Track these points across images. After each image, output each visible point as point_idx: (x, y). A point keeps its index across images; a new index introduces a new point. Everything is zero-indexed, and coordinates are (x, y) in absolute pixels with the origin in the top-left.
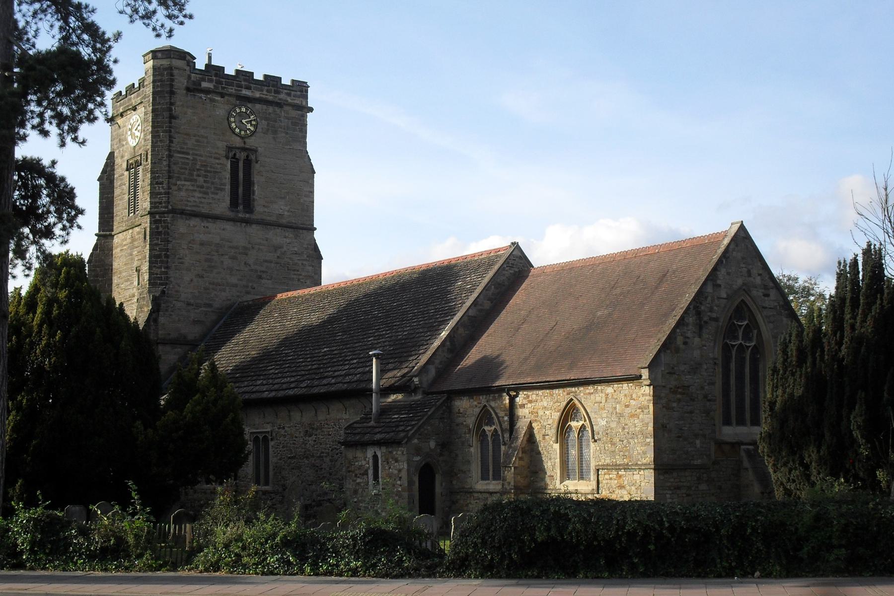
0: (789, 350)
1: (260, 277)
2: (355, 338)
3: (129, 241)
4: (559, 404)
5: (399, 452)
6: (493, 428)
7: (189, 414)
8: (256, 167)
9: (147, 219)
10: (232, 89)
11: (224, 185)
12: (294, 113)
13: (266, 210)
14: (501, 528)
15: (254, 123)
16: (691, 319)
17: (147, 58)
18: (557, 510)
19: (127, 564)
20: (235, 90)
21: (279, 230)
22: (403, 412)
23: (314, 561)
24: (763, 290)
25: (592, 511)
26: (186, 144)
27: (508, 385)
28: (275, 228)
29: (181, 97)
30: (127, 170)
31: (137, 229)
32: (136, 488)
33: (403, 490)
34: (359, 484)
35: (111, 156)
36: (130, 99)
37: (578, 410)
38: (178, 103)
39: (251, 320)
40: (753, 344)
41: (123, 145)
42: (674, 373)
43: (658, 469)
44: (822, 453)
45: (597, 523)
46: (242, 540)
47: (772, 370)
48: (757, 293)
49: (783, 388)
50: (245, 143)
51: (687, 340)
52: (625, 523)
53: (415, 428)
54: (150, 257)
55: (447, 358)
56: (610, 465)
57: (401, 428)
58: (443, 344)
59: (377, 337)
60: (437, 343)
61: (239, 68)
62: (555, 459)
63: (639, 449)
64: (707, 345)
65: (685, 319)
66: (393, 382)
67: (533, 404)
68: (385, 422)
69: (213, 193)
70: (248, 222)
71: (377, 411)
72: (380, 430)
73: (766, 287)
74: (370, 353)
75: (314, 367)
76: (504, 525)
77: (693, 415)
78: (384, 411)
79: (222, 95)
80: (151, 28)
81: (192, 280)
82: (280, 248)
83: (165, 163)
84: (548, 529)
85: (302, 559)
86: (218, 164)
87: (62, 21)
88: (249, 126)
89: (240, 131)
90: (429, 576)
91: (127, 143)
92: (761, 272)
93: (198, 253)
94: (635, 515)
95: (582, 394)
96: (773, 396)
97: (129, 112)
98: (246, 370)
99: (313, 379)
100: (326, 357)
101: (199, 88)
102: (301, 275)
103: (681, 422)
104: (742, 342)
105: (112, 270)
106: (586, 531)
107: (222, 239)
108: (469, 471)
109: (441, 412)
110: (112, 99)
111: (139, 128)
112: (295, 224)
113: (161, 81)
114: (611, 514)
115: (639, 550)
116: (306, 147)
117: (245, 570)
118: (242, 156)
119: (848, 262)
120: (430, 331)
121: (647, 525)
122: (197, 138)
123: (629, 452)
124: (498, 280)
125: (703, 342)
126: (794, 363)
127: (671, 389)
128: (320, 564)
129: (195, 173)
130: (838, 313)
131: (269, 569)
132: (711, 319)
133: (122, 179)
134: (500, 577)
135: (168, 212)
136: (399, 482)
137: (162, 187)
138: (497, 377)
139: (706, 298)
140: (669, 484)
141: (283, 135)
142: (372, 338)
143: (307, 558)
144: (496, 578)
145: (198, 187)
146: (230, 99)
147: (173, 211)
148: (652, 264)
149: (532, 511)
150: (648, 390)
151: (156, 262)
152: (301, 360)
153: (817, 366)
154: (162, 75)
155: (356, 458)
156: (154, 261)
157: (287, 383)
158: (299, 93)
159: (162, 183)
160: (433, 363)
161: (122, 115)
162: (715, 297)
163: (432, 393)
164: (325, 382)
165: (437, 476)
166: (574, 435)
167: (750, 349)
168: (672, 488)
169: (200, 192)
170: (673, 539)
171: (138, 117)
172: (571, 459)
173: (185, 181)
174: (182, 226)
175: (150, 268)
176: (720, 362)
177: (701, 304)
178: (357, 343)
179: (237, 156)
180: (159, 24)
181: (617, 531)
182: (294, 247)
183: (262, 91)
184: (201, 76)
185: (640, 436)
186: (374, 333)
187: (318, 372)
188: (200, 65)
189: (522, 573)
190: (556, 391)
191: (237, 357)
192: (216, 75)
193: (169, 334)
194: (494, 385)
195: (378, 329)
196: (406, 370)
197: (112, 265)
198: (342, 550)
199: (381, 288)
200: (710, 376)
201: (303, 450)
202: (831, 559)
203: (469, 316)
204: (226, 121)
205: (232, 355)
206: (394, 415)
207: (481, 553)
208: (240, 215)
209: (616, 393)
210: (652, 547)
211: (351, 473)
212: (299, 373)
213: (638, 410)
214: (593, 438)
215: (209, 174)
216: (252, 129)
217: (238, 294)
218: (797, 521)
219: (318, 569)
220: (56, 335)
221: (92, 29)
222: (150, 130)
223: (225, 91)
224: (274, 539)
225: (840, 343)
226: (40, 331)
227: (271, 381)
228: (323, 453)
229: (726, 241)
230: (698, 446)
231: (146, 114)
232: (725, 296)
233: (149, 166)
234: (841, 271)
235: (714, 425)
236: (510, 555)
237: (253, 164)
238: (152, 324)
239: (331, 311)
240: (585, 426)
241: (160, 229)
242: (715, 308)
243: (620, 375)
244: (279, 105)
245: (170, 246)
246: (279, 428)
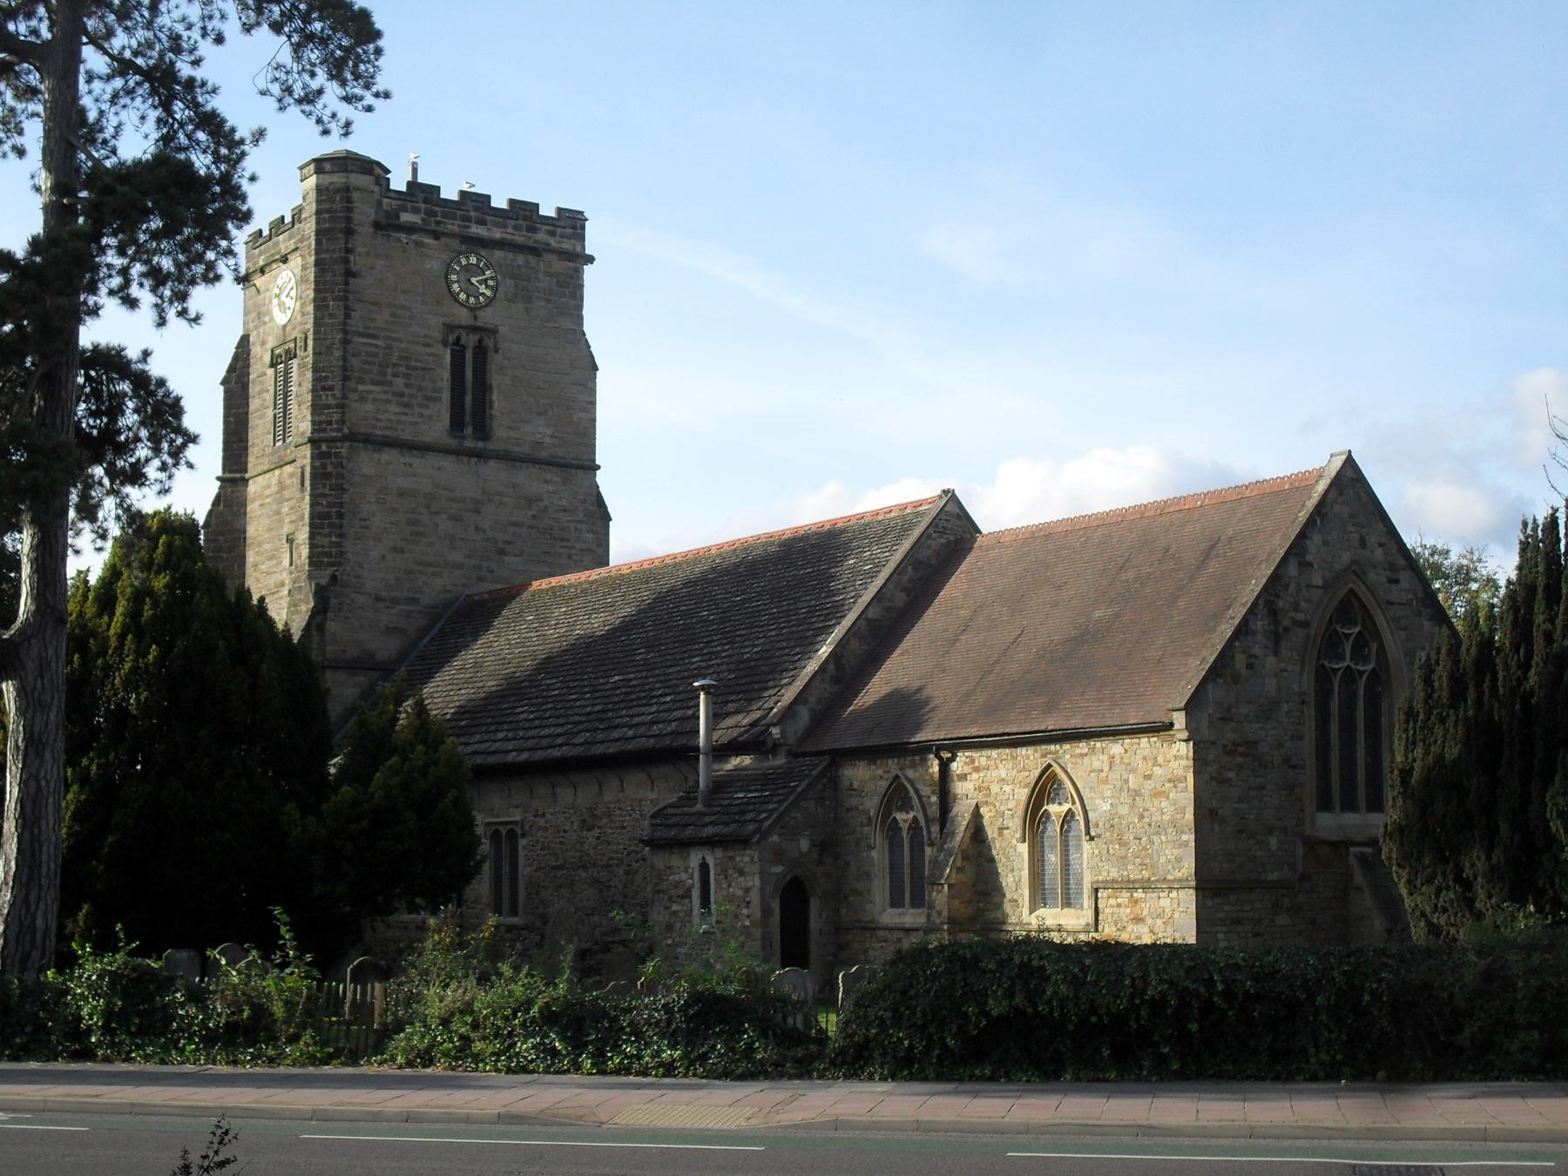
0: (1435, 677)
1: (502, 552)
2: (669, 657)
3: (274, 489)
4: (1027, 774)
5: (746, 858)
6: (911, 816)
7: (380, 792)
8: (495, 361)
9: (307, 451)
10: (453, 224)
11: (439, 390)
12: (561, 266)
13: (512, 434)
14: (928, 991)
15: (491, 283)
16: (1260, 623)
17: (306, 171)
18: (1025, 960)
19: (271, 1052)
20: (459, 226)
21: (534, 470)
22: (752, 788)
23: (597, 1049)
24: (1388, 573)
25: (1088, 962)
26: (374, 320)
27: (938, 740)
28: (527, 467)
29: (364, 239)
30: (273, 365)
31: (288, 469)
32: (288, 919)
33: (753, 924)
34: (675, 913)
35: (244, 343)
36: (277, 243)
37: (1060, 784)
38: (360, 249)
39: (486, 626)
40: (1370, 667)
41: (265, 323)
42: (1231, 719)
43: (1203, 889)
44: (1495, 860)
45: (1095, 983)
46: (472, 1012)
47: (1406, 713)
48: (1376, 577)
49: (1424, 744)
50: (475, 318)
51: (1253, 660)
52: (1147, 984)
53: (775, 816)
54: (312, 517)
55: (830, 693)
56: (1117, 882)
57: (749, 816)
58: (823, 668)
59: (707, 657)
60: (812, 667)
61: (465, 188)
62: (1021, 870)
63: (1170, 853)
64: (1289, 669)
65: (1251, 624)
66: (735, 735)
67: (982, 774)
68: (721, 805)
69: (421, 406)
70: (481, 456)
71: (707, 787)
72: (713, 818)
73: (1392, 567)
74: (696, 684)
75: (596, 709)
76: (931, 987)
77: (1264, 792)
78: (720, 786)
79: (436, 235)
80: (314, 118)
81: (383, 557)
82: (536, 501)
83: (337, 354)
84: (1010, 995)
85: (578, 1045)
86: (429, 355)
87: (161, 109)
88: (482, 289)
89: (468, 297)
90: (799, 1077)
91: (272, 320)
92: (1384, 540)
93: (395, 510)
94: (1164, 969)
95: (1067, 757)
96: (1407, 758)
97: (274, 266)
98: (478, 714)
99: (596, 730)
100: (618, 692)
101: (397, 222)
102: (573, 548)
103: (1244, 806)
104: (1353, 666)
105: (245, 539)
106: (1076, 997)
107: (436, 486)
108: (869, 891)
109: (820, 787)
110: (246, 243)
111: (293, 293)
112: (564, 458)
113: (329, 211)
114: (1122, 967)
115: (1170, 1031)
116: (581, 325)
117: (477, 1064)
118: (470, 340)
119: (1541, 521)
120: (799, 646)
121: (1185, 988)
122: (394, 310)
123: (1152, 859)
124: (920, 556)
125: (1282, 665)
126: (1445, 700)
127: (1225, 746)
128: (609, 1055)
129: (390, 371)
130: (1522, 611)
131: (519, 1062)
132: (1296, 623)
133: (262, 382)
134: (925, 1079)
135: (345, 438)
136: (745, 911)
137: (333, 396)
138: (918, 727)
139: (1288, 585)
140: (1222, 915)
141: (543, 303)
142: (698, 658)
143: (586, 1044)
144: (917, 1080)
145: (394, 394)
146: (449, 241)
147: (352, 437)
148: (1189, 528)
149: (982, 962)
150: (1184, 750)
151: (321, 526)
152: (574, 696)
153: (1485, 707)
154: (333, 201)
155: (670, 867)
156: (318, 522)
157: (550, 736)
158: (569, 231)
159: (331, 389)
160: (805, 702)
161: (262, 271)
162: (1304, 585)
163: (804, 755)
164: (616, 734)
165: (812, 901)
166: (1054, 829)
167: (1365, 676)
168: (1228, 922)
169: (398, 403)
170: (1230, 1013)
171: (291, 274)
172: (1049, 870)
174: (366, 463)
175: (312, 536)
176: (1311, 698)
177: (1278, 597)
178: (670, 666)
179: (463, 342)
180: (328, 112)
181: (1132, 997)
182: (560, 499)
183: (505, 227)
184: (399, 202)
185: (1171, 830)
186: (702, 648)
187: (604, 716)
188: (398, 183)
189: (964, 1072)
190: (1022, 751)
191: (463, 691)
192: (425, 201)
193: (344, 651)
194: (912, 740)
195: (709, 642)
196: (758, 714)
197: (245, 532)
198: (647, 1030)
199: (713, 569)
200: (1293, 723)
201: (578, 854)
202: (1514, 1047)
203: (867, 619)
204: (443, 280)
205: (454, 687)
206: (737, 793)
207: (891, 1036)
208: (469, 444)
209: (1128, 755)
210: (1194, 1027)
211: (661, 895)
212: (572, 719)
213: (1168, 785)
214: (1088, 832)
216: (488, 293)
217: (464, 581)
218: (1451, 981)
219: (605, 1062)
220: (149, 653)
221: (212, 123)
222: (312, 296)
223: (440, 228)
224: (527, 1011)
225: (1525, 666)
226: (121, 646)
227: (521, 733)
228: (611, 859)
229: (1322, 487)
230: (1274, 848)
231: (304, 268)
232: (1320, 583)
233: (310, 360)
234: (1527, 538)
235: (1303, 811)
236: (943, 1039)
237: (491, 354)
238: (315, 633)
239: (623, 613)
240: (1073, 813)
241: (330, 469)
242: (1303, 604)
243: (1135, 721)
244: (535, 251)
245: (346, 498)
246: (535, 816)
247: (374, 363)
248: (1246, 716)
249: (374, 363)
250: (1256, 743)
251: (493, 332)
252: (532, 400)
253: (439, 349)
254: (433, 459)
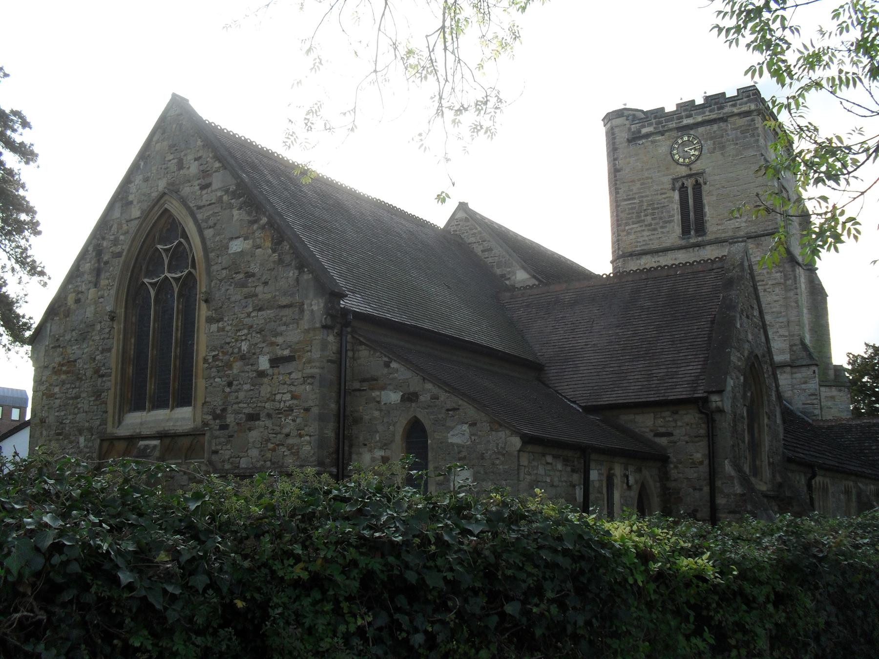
8: (705, 188)
26: (632, 190)
42: (59, 346)
50: (691, 169)
69: (662, 227)
86: (665, 198)
88: (692, 152)
89: (684, 159)
102: (767, 284)
127: (54, 368)
129: (642, 214)
141: (732, 147)
145: (646, 226)
169: (649, 230)
173: (633, 224)
204: (670, 156)
208: (692, 241)
215: (656, 211)
244: (723, 120)
247: (633, 213)
248: (70, 341)
249: (633, 213)
250: (75, 361)
251: (702, 173)
252: (730, 204)
253: (670, 193)
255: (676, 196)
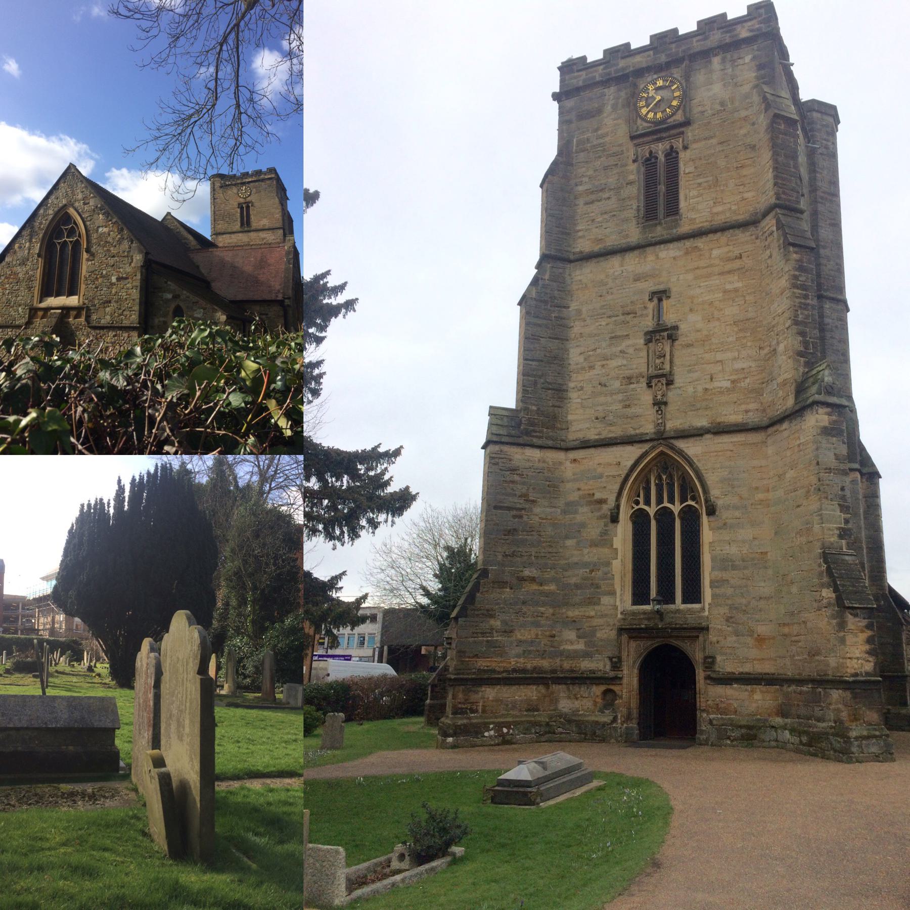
8: (251, 208)
118: (244, 206)
208: (246, 229)
254: (236, 235)
255: (239, 210)
